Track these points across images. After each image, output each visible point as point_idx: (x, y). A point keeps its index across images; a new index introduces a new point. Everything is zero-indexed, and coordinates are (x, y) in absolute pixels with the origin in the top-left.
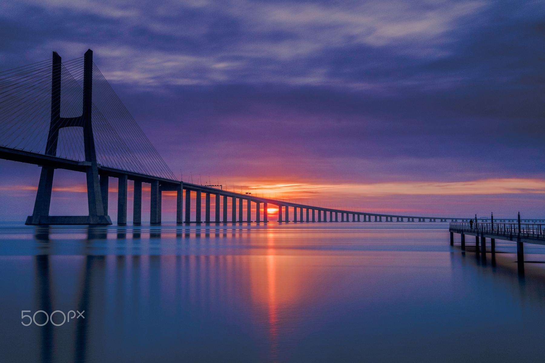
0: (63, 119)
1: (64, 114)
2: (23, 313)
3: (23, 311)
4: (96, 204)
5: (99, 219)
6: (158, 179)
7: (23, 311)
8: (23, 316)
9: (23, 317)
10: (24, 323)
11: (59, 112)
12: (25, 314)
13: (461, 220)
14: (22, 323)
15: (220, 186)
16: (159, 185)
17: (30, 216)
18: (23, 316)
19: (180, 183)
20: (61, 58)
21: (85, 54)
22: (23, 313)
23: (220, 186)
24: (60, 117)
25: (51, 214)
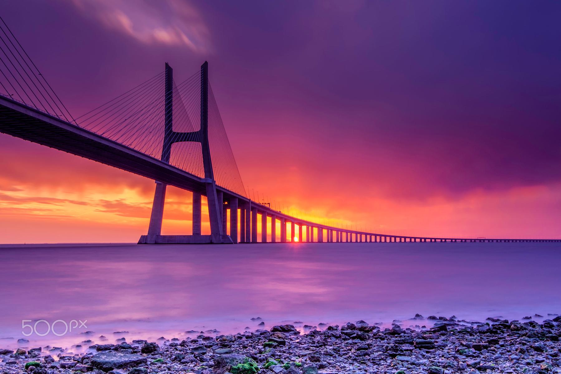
0: (174, 133)
1: (177, 128)
2: (24, 322)
3: (23, 321)
4: (218, 223)
5: (222, 239)
6: (238, 197)
7: (23, 321)
8: (24, 325)
9: (23, 327)
10: (25, 333)
11: (171, 126)
12: (25, 323)
13: (440, 240)
14: (23, 332)
15: (268, 204)
16: (224, 202)
17: (144, 236)
18: (24, 325)
19: (249, 201)
20: (172, 69)
21: (202, 67)
22: (24, 322)
23: (268, 204)
24: (171, 131)
25: (162, 234)
